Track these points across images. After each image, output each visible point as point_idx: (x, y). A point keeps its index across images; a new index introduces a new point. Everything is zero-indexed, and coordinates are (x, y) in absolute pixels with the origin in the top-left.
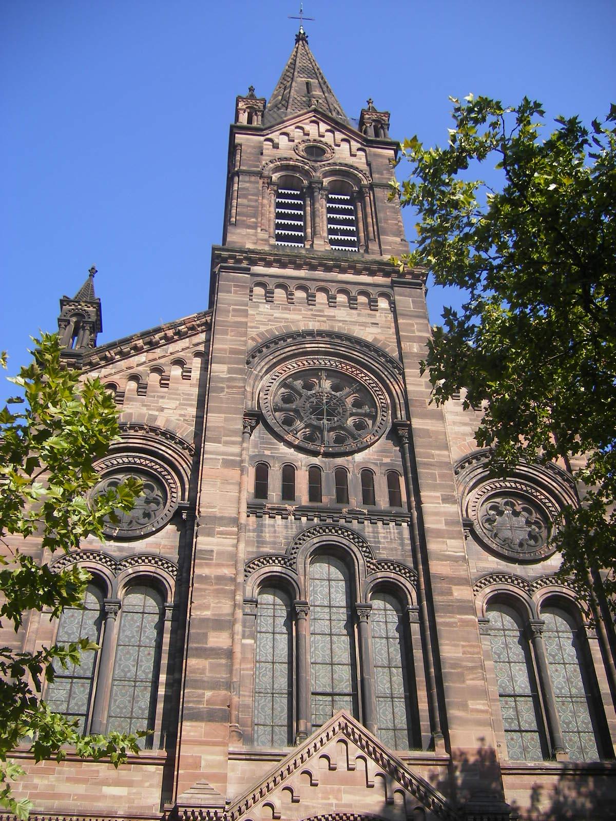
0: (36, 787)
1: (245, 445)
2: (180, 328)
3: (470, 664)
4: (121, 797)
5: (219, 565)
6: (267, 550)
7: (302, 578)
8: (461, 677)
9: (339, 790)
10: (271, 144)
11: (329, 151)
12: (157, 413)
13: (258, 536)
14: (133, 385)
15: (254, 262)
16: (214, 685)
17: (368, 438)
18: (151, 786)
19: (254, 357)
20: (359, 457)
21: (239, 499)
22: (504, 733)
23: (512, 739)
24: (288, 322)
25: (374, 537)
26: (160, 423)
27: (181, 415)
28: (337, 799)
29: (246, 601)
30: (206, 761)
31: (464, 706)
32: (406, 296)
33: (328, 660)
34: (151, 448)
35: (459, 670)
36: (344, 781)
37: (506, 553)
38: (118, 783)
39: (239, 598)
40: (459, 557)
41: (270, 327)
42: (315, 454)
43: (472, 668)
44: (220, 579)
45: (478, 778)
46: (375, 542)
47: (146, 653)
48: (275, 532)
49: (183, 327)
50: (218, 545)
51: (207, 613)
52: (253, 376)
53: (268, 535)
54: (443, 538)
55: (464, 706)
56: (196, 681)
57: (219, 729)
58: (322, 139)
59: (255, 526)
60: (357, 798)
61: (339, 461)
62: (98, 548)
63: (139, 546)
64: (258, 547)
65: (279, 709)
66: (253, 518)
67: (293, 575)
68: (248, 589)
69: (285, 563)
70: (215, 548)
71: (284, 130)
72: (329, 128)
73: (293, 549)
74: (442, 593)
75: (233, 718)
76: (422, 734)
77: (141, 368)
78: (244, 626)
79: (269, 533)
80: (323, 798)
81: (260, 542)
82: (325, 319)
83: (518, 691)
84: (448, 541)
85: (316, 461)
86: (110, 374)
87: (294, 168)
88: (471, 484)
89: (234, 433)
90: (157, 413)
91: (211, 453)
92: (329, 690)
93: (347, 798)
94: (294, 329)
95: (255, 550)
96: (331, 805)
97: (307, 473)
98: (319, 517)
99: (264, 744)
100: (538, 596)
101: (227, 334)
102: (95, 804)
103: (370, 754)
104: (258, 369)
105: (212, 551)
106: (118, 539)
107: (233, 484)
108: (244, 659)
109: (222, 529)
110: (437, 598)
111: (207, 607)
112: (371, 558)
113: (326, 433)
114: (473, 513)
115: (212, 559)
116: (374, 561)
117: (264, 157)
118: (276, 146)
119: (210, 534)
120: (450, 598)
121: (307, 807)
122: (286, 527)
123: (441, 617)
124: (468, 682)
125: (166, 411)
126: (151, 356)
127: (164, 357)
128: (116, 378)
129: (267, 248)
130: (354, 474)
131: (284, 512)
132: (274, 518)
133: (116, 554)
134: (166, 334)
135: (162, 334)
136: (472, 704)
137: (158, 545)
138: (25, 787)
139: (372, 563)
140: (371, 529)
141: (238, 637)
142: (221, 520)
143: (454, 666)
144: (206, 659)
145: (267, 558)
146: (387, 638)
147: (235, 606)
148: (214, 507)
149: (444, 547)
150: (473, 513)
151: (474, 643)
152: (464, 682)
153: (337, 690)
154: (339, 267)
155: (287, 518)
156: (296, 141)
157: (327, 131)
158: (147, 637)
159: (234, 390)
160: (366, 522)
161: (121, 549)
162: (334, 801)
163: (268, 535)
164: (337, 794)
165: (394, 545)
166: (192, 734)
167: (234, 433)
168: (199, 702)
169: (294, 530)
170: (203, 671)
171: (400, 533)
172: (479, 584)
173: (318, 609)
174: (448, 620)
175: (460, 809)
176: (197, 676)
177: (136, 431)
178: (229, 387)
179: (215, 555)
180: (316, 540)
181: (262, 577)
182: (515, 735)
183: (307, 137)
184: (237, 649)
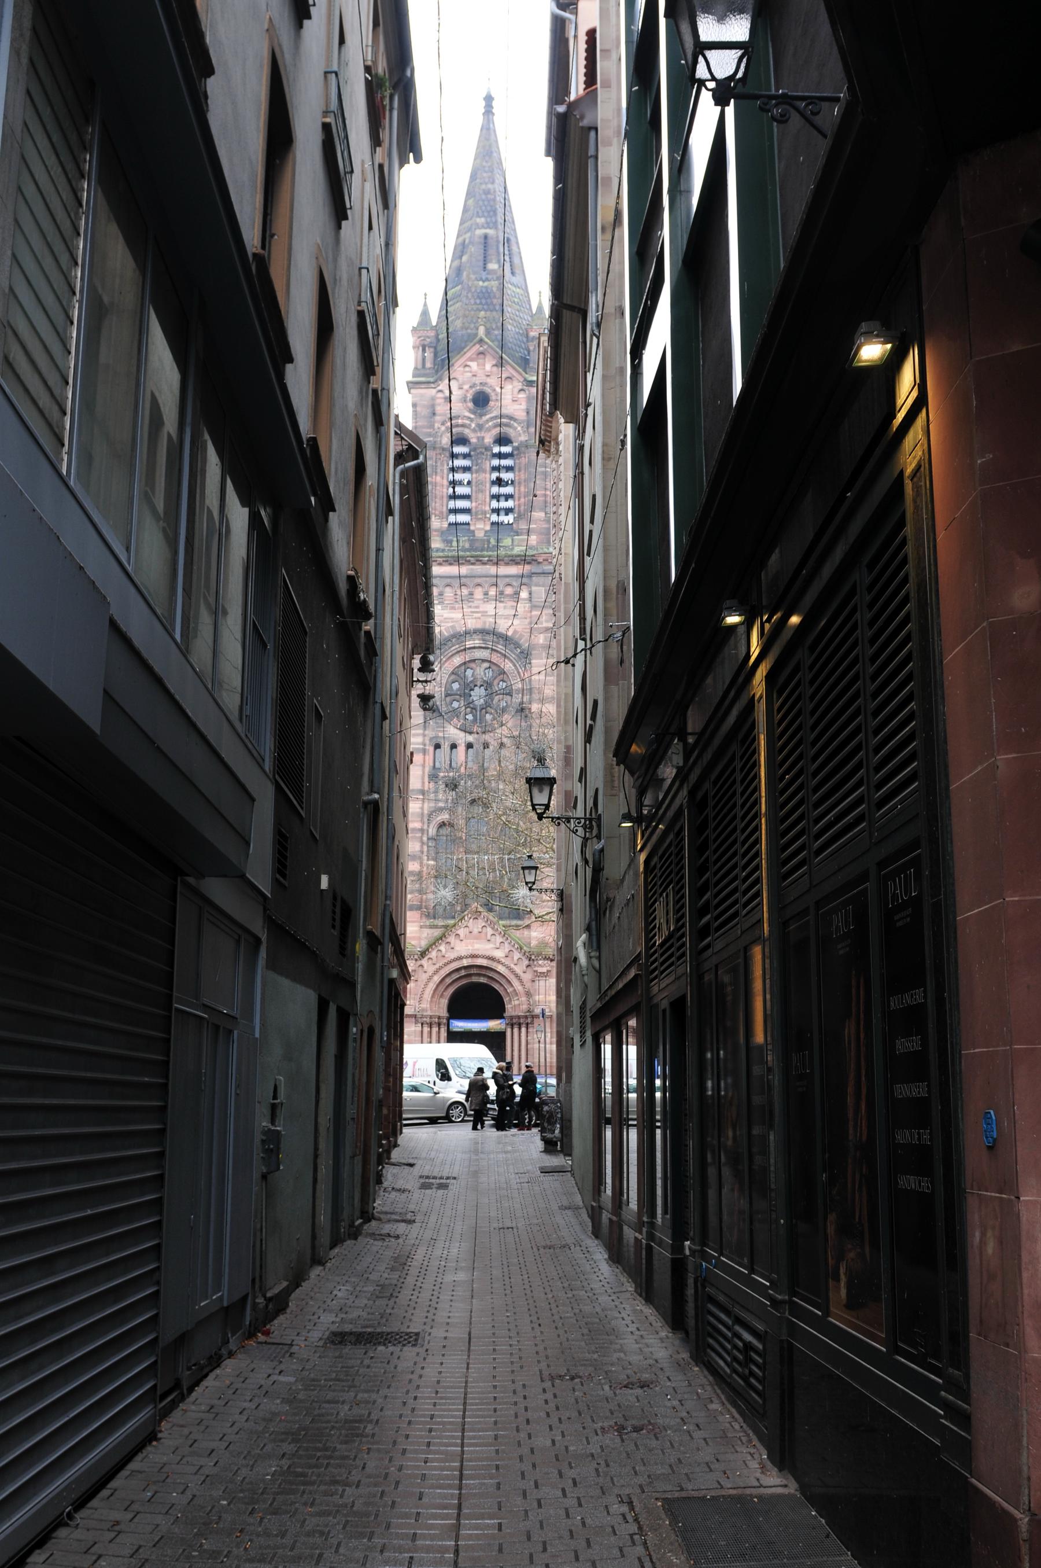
21: (424, 773)
32: (539, 586)
36: (476, 938)
39: (425, 839)
42: (471, 733)
68: (430, 830)
82: (479, 615)
93: (477, 946)
94: (458, 629)
117: (437, 418)
141: (425, 862)
147: (423, 843)
154: (491, 561)
162: (471, 948)
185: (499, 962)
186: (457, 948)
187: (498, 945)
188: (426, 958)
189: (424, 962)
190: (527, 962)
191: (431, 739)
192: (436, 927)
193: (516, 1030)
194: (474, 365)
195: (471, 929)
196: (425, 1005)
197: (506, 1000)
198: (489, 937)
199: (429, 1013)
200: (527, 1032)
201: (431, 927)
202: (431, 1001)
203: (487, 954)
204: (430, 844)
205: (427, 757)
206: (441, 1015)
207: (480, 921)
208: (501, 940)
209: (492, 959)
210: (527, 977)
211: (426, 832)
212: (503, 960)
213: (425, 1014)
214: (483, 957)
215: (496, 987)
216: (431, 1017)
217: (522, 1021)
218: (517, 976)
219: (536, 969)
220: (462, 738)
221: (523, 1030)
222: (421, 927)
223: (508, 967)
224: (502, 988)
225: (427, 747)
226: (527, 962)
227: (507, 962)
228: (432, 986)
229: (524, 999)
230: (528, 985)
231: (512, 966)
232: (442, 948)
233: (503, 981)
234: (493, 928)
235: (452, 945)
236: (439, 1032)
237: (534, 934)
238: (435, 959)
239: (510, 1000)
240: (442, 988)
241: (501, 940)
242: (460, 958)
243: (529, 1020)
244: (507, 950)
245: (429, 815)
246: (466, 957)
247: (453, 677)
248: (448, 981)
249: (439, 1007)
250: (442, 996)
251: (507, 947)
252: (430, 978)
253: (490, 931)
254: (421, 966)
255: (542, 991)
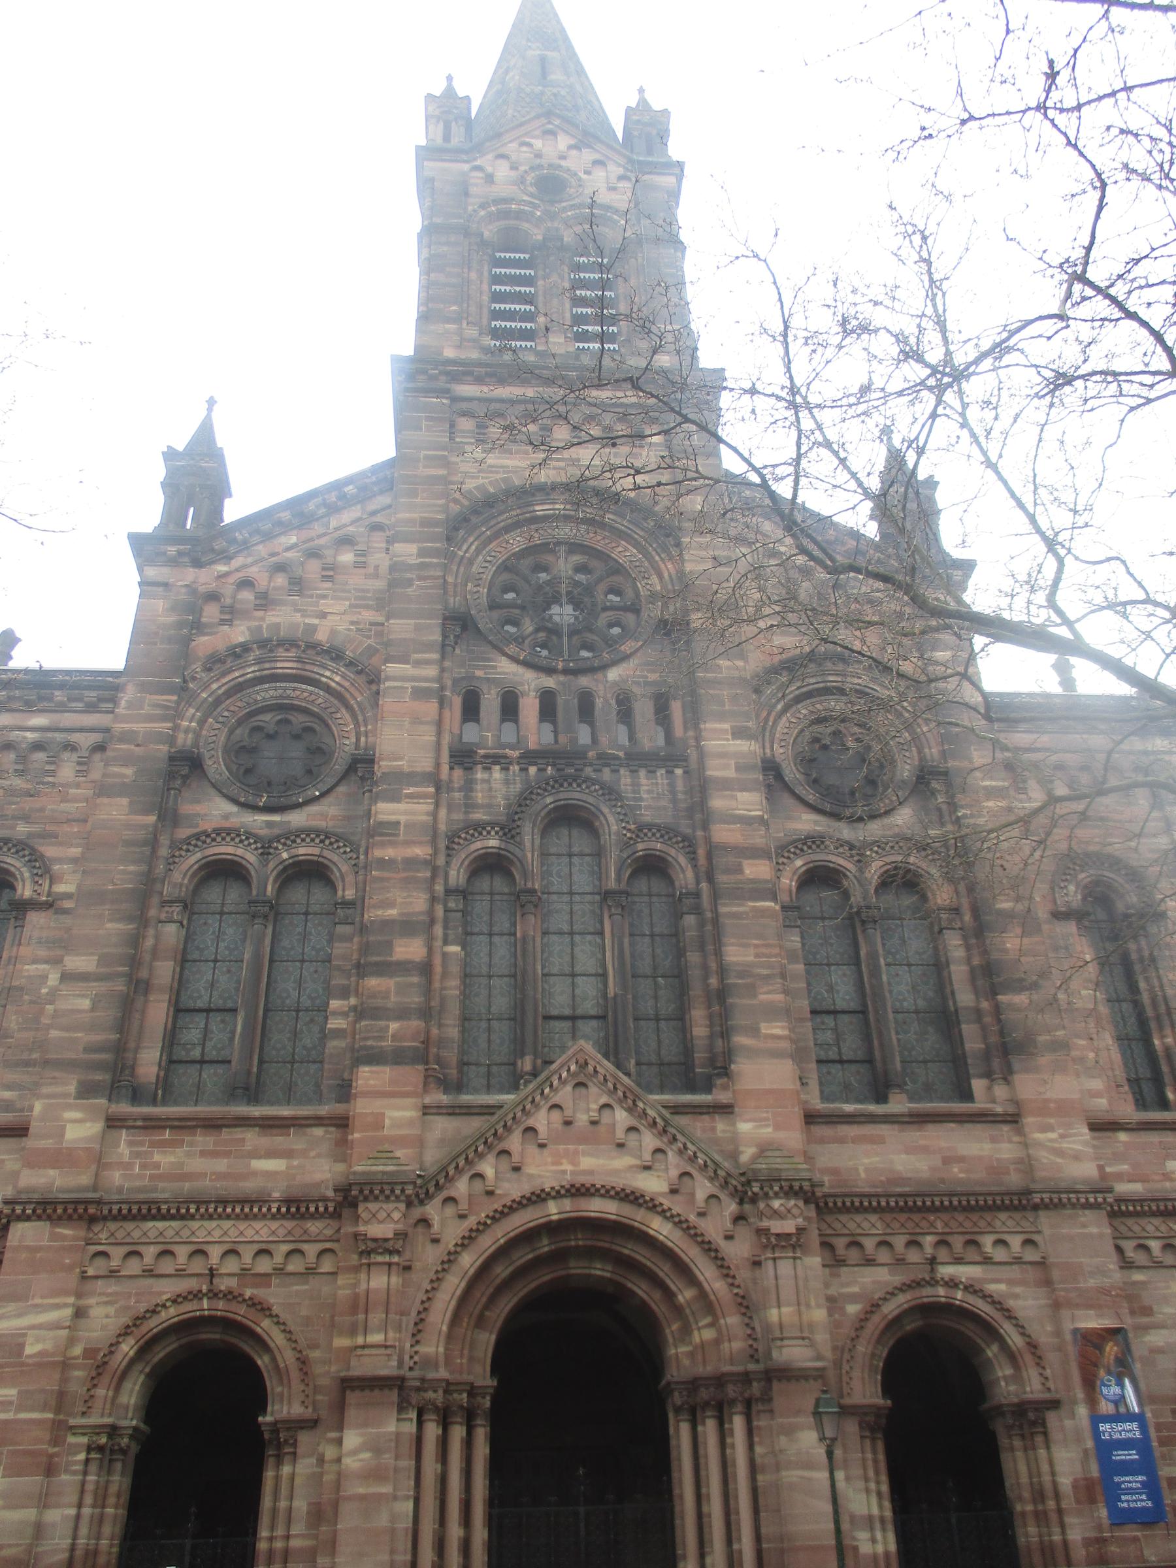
0: (157, 1166)
1: (447, 664)
2: (346, 489)
3: (765, 972)
4: (276, 1173)
5: (408, 843)
6: (479, 816)
7: (529, 855)
8: (752, 990)
9: (576, 1152)
10: (481, 175)
11: (574, 183)
12: (316, 621)
13: (467, 797)
14: (281, 580)
15: (455, 378)
16: (402, 1014)
17: (627, 647)
18: (319, 1156)
19: (456, 529)
20: (613, 674)
22: (814, 1065)
23: (829, 1073)
24: (508, 472)
25: (634, 792)
26: (322, 636)
27: (352, 623)
28: (573, 1164)
29: (448, 892)
30: (391, 1118)
31: (754, 1031)
33: (567, 970)
34: (309, 674)
35: (749, 981)
36: (583, 1139)
37: (828, 807)
38: (271, 1154)
39: (439, 888)
40: (754, 817)
41: (481, 481)
42: (550, 671)
43: (768, 977)
44: (410, 863)
45: (770, 1130)
46: (635, 799)
47: (312, 969)
48: (490, 789)
49: (351, 487)
50: (406, 813)
51: (393, 912)
52: (457, 560)
53: (480, 795)
54: (732, 789)
55: (754, 1031)
56: (376, 1008)
57: (413, 1074)
58: (563, 163)
59: (462, 782)
60: (601, 1162)
61: (584, 681)
62: (238, 826)
63: (297, 819)
64: (466, 813)
65: (498, 1041)
66: (458, 773)
67: (517, 851)
68: (453, 873)
69: (505, 834)
70: (402, 819)
71: (502, 151)
72: (572, 142)
73: (516, 813)
74: (727, 871)
75: (431, 1058)
76: (697, 1070)
77: (289, 555)
78: (446, 927)
79: (482, 791)
80: (554, 1164)
81: (470, 806)
82: (562, 464)
83: (841, 1004)
84: (739, 795)
85: (550, 682)
86: (245, 566)
87: (519, 215)
88: (779, 707)
89: (427, 647)
90: (316, 621)
91: (395, 679)
92: (567, 1012)
95: (461, 817)
96: (564, 1172)
97: (537, 701)
98: (554, 765)
99: (476, 1091)
100: (874, 870)
101: (416, 497)
102: (241, 1184)
103: (620, 1101)
104: (464, 548)
105: (398, 823)
106: (269, 809)
107: (427, 723)
108: (445, 975)
109: (412, 790)
110: (722, 879)
111: (391, 904)
112: (628, 822)
113: (565, 639)
114: (782, 751)
115: (398, 835)
116: (633, 827)
117: (471, 200)
118: (490, 179)
119: (395, 798)
120: (739, 877)
121: (531, 1176)
122: (507, 782)
123: (725, 905)
124: (762, 997)
125: (329, 617)
126: (305, 534)
127: (324, 535)
128: (253, 572)
129: (475, 355)
130: (606, 701)
131: (503, 761)
132: (490, 769)
133: (263, 832)
134: (324, 500)
135: (319, 500)
136: (767, 1029)
137: (324, 816)
138: (143, 1166)
139: (629, 830)
140: (629, 780)
141: (438, 943)
142: (410, 778)
143: (742, 974)
144: (391, 977)
145: (479, 828)
146: (652, 936)
147: (433, 899)
148: (401, 759)
149: (733, 804)
150: (782, 751)
151: (771, 942)
152: (755, 996)
153: (579, 1012)
155: (507, 769)
156: (522, 168)
157: (570, 147)
158: (313, 948)
159: (429, 583)
160: (622, 771)
161: (269, 824)
162: (568, 1167)
163: (480, 795)
164: (573, 1159)
165: (663, 803)
166: (372, 1082)
167: (427, 647)
168: (381, 1038)
169: (519, 786)
170: (386, 995)
171: (672, 785)
172: (786, 854)
173: (554, 897)
174: (735, 909)
175: (743, 1174)
176: (379, 1002)
177: (287, 650)
178: (420, 578)
179: (402, 828)
180: (549, 800)
181: (472, 857)
182: (835, 1069)
183: (538, 161)
184: (437, 961)
185: (652, 1205)
186: (530, 1169)
187: (647, 1156)
188: (437, 1201)
189: (432, 1210)
190: (732, 1207)
191: (456, 682)
192: (468, 1111)
193: (709, 1428)
194: (538, 144)
195: (568, 1112)
196: (432, 1347)
197: (672, 1329)
198: (620, 1134)
199: (443, 1373)
200: (750, 1432)
201: (454, 1111)
202: (450, 1337)
203: (619, 1182)
204: (452, 905)
205: (447, 713)
206: (479, 1383)
207: (593, 1090)
208: (657, 1143)
209: (632, 1198)
210: (739, 1250)
211: (441, 873)
212: (667, 1203)
213: (431, 1375)
214: (608, 1193)
215: (641, 1289)
216: (449, 1387)
217: (731, 1391)
218: (709, 1249)
219: (765, 1223)
220: (530, 683)
221: (738, 1423)
222: (426, 1110)
223: (680, 1223)
224: (657, 1295)
225: (448, 693)
226: (732, 1207)
227: (677, 1206)
228: (454, 1284)
229: (732, 1320)
230: (743, 1274)
231: (692, 1218)
232: (488, 1168)
233: (664, 1270)
234: (630, 1110)
235: (516, 1158)
236: (468, 1443)
237: (744, 1127)
238: (463, 1206)
239: (686, 1330)
240: (482, 1294)
241: (657, 1143)
242: (538, 1198)
243: (756, 1388)
244: (674, 1173)
245: (452, 838)
246: (558, 1195)
247: (505, 576)
248: (502, 1271)
249: (471, 1359)
250: (480, 1322)
251: (674, 1163)
252: (450, 1260)
253: (621, 1117)
254: (425, 1222)
255: (787, 1291)
